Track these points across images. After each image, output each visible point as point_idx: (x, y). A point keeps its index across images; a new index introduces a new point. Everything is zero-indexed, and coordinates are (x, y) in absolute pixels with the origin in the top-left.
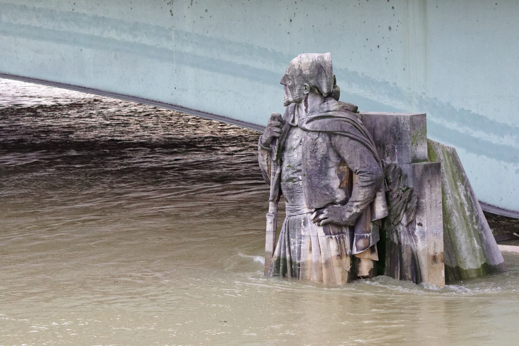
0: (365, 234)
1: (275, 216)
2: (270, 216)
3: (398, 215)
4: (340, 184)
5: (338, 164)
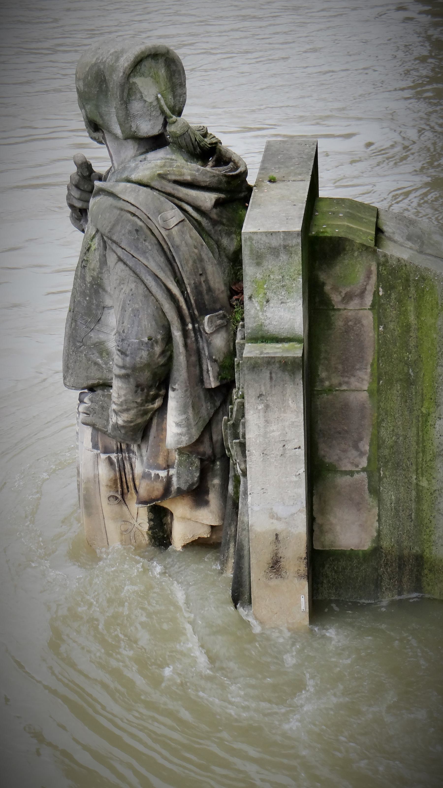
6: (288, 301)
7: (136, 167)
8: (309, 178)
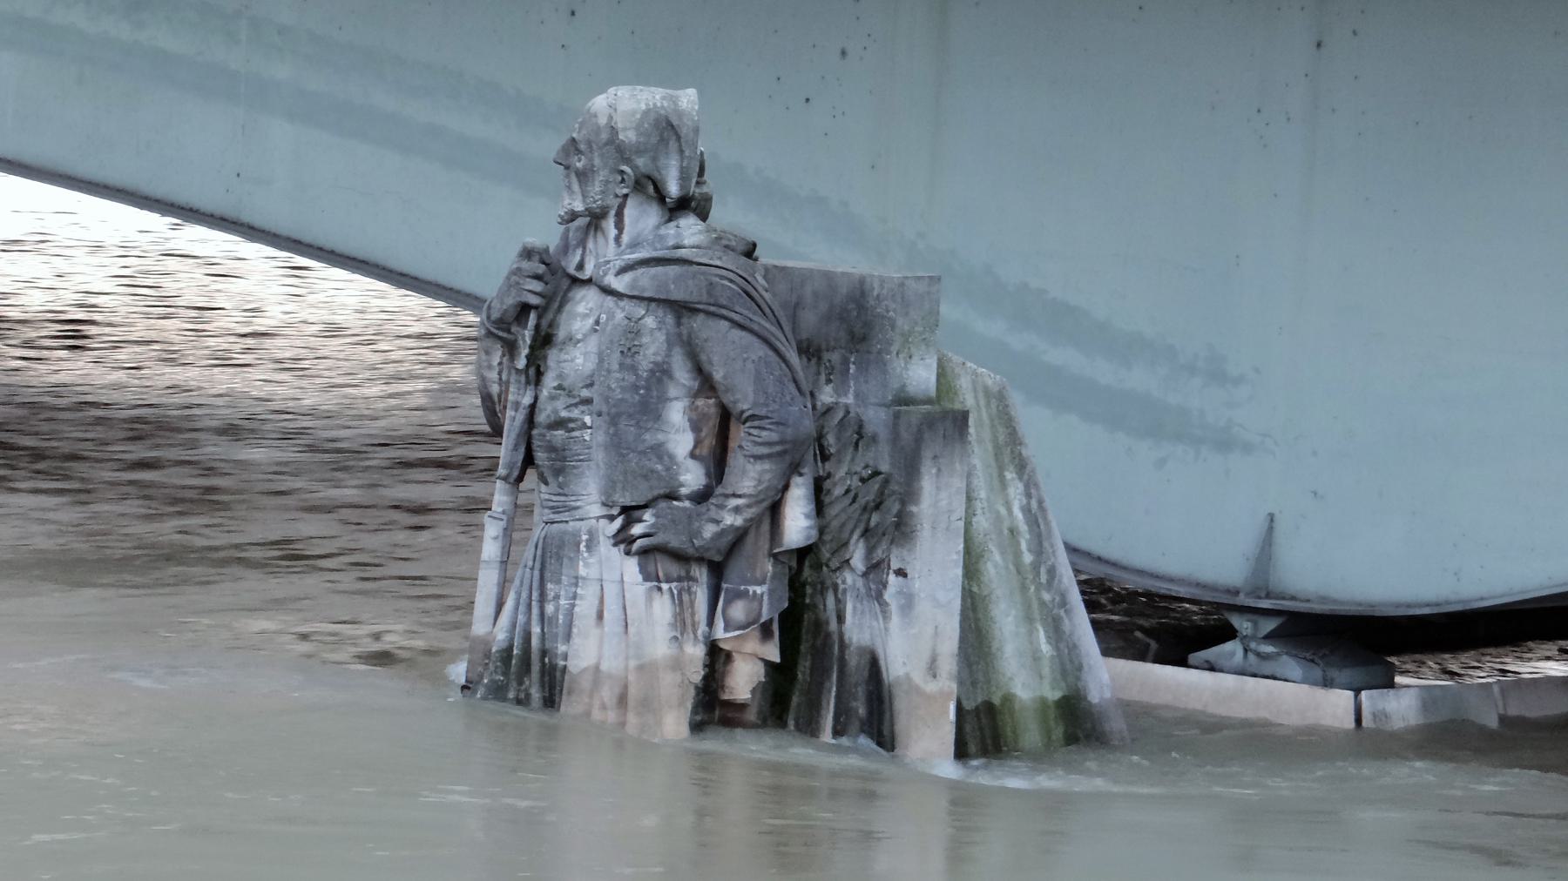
0: (749, 585)
1: (508, 521)
2: (495, 518)
3: (844, 542)
4: (695, 447)
5: (692, 392)
6: (926, 357)
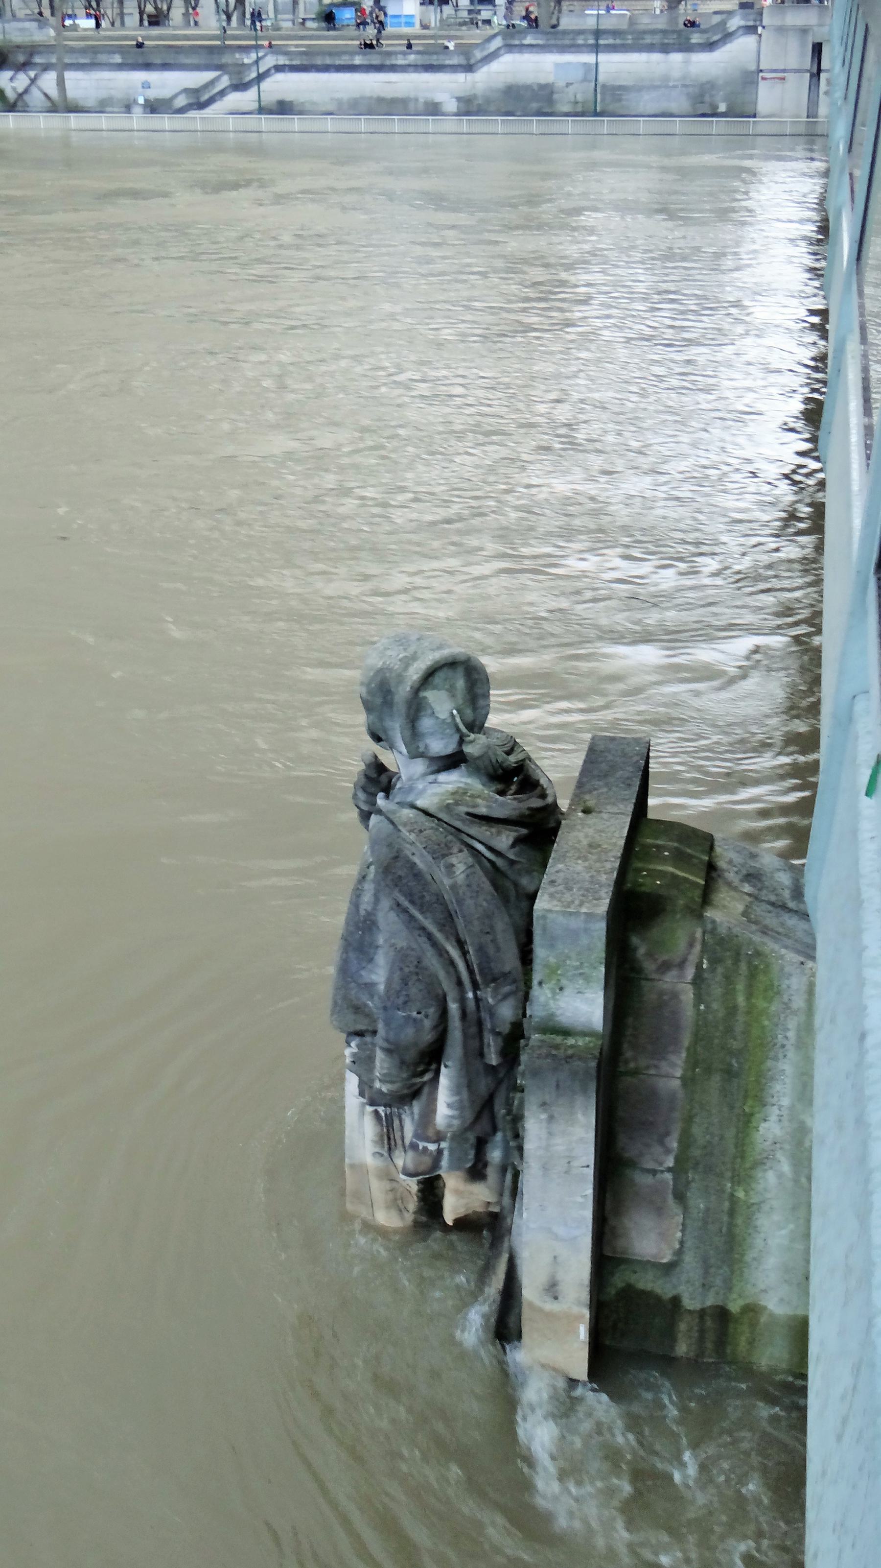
7: (423, 791)
8: (630, 808)
